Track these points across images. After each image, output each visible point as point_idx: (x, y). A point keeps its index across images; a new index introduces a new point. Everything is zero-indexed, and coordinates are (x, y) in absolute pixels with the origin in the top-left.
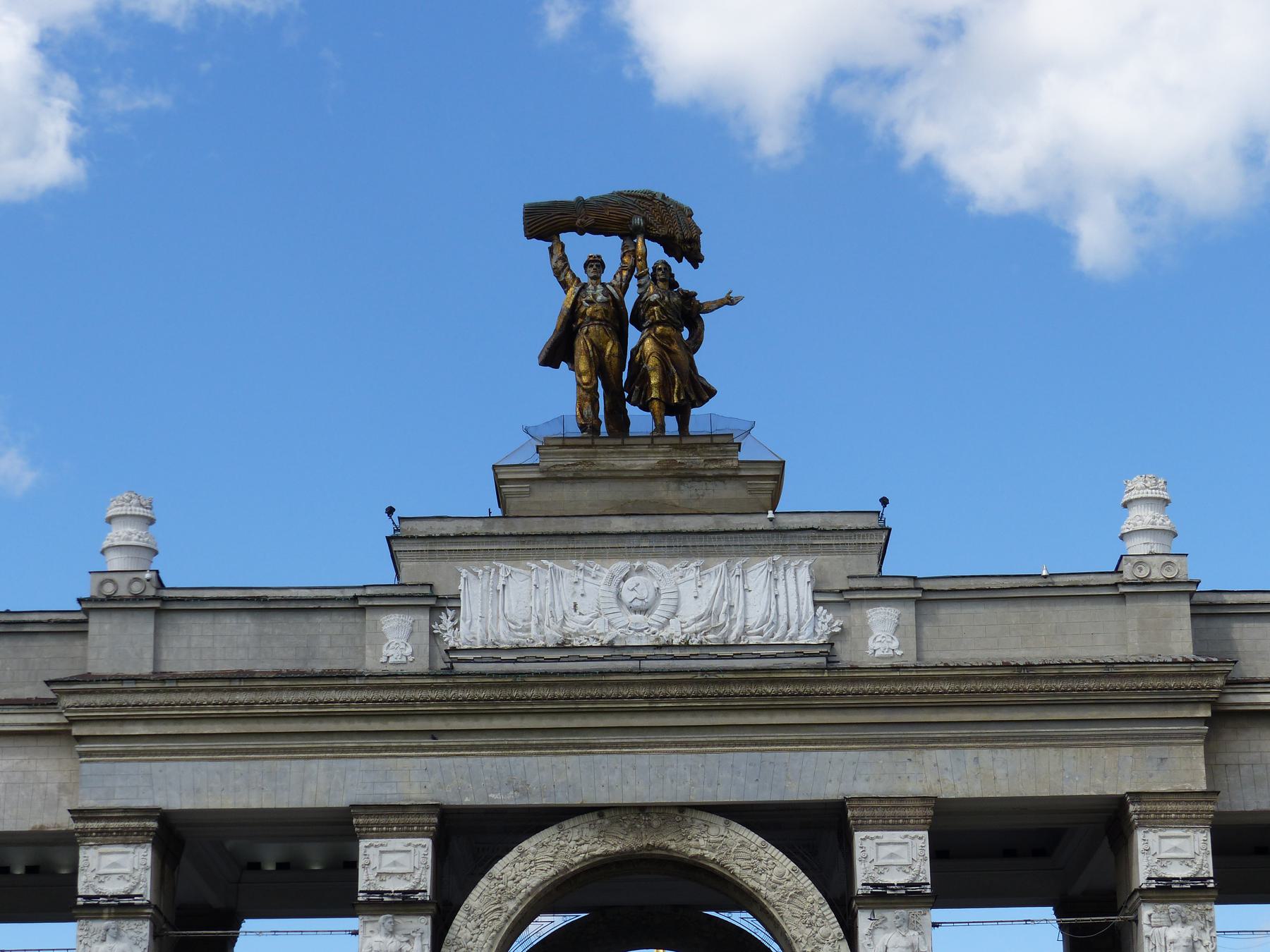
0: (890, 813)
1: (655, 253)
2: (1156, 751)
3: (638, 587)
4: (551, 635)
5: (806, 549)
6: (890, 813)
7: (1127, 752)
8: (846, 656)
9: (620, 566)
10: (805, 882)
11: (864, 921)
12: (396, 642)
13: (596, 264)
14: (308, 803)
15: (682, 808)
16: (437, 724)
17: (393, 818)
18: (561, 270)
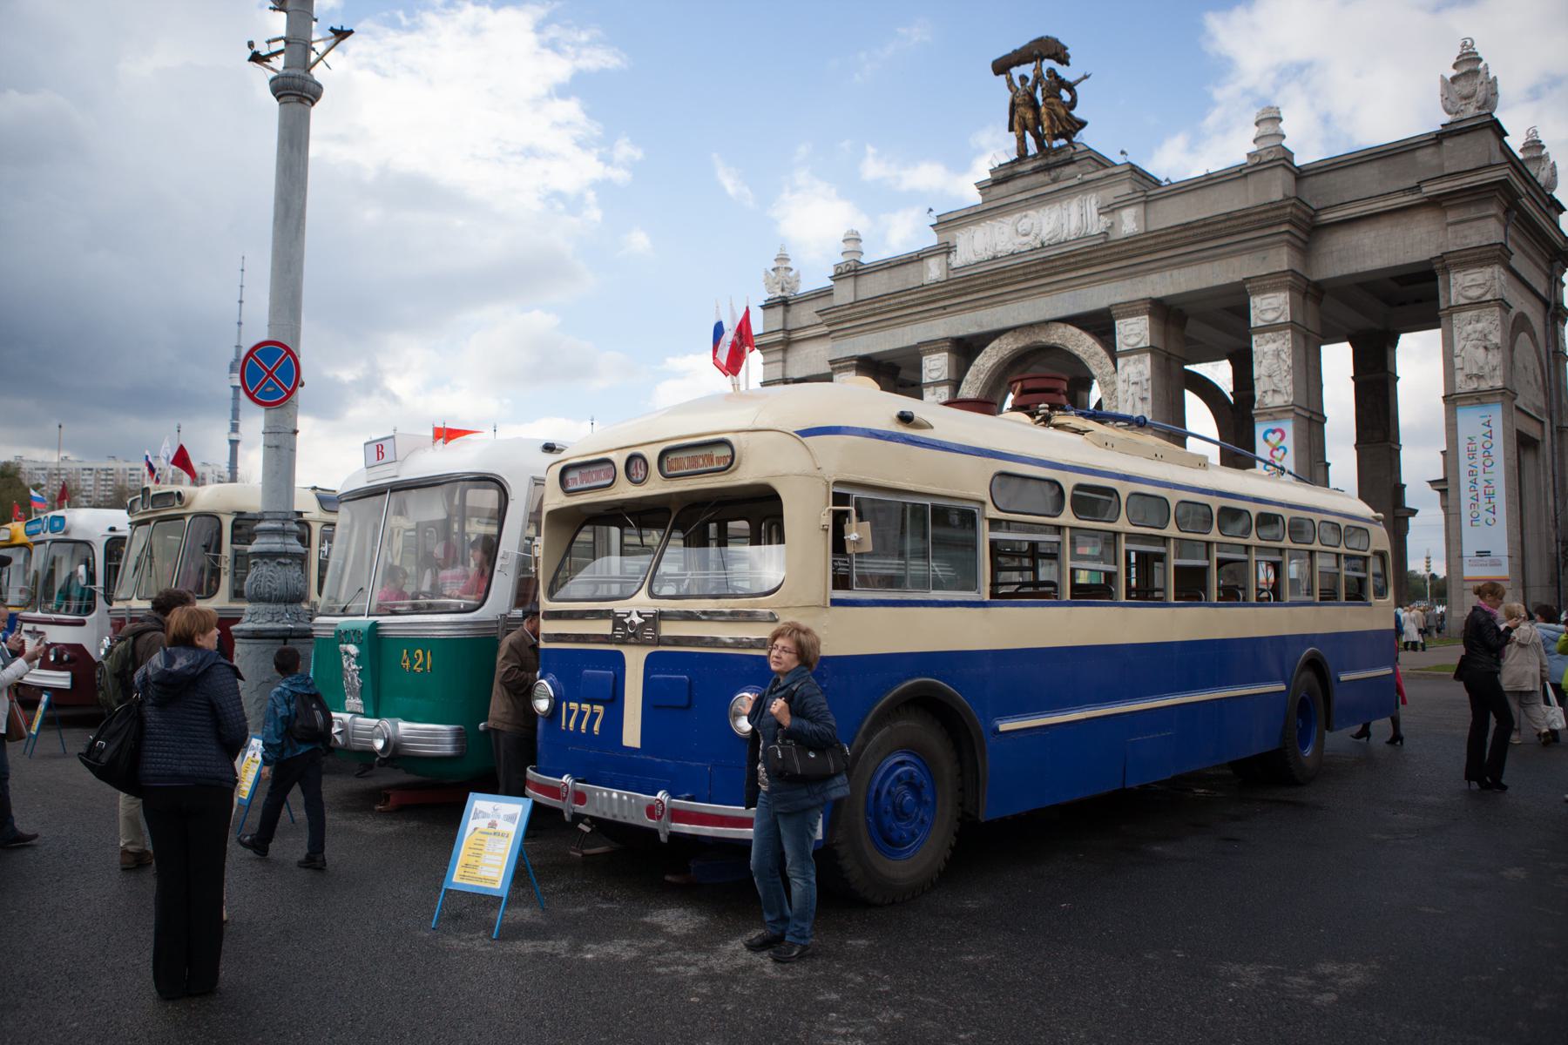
0: (1130, 309)
1: (1048, 64)
2: (1261, 254)
3: (1025, 224)
4: (990, 254)
5: (1096, 189)
6: (1130, 309)
7: (1246, 257)
8: (1114, 236)
9: (1017, 216)
10: (1098, 348)
11: (1120, 361)
12: (934, 271)
13: (1024, 78)
14: (905, 344)
15: (1047, 322)
16: (946, 303)
17: (932, 346)
18: (1010, 82)
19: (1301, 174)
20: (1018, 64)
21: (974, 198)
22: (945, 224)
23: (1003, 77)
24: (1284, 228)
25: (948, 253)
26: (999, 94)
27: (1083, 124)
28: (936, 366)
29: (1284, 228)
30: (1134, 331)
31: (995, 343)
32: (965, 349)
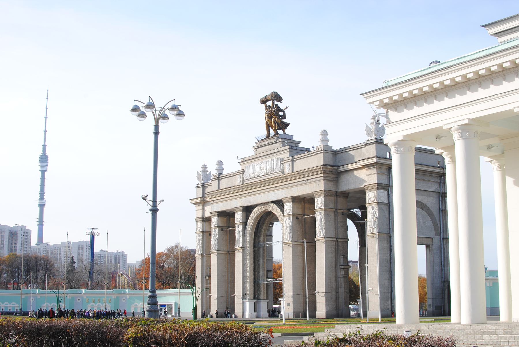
1: (276, 103)
10: (281, 213)
19: (335, 153)
20: (268, 100)
21: (251, 153)
22: (243, 161)
23: (264, 105)
24: (322, 175)
25: (243, 174)
26: (262, 111)
27: (287, 125)
28: (239, 216)
29: (322, 175)
30: (288, 207)
31: (256, 208)
32: (248, 210)
